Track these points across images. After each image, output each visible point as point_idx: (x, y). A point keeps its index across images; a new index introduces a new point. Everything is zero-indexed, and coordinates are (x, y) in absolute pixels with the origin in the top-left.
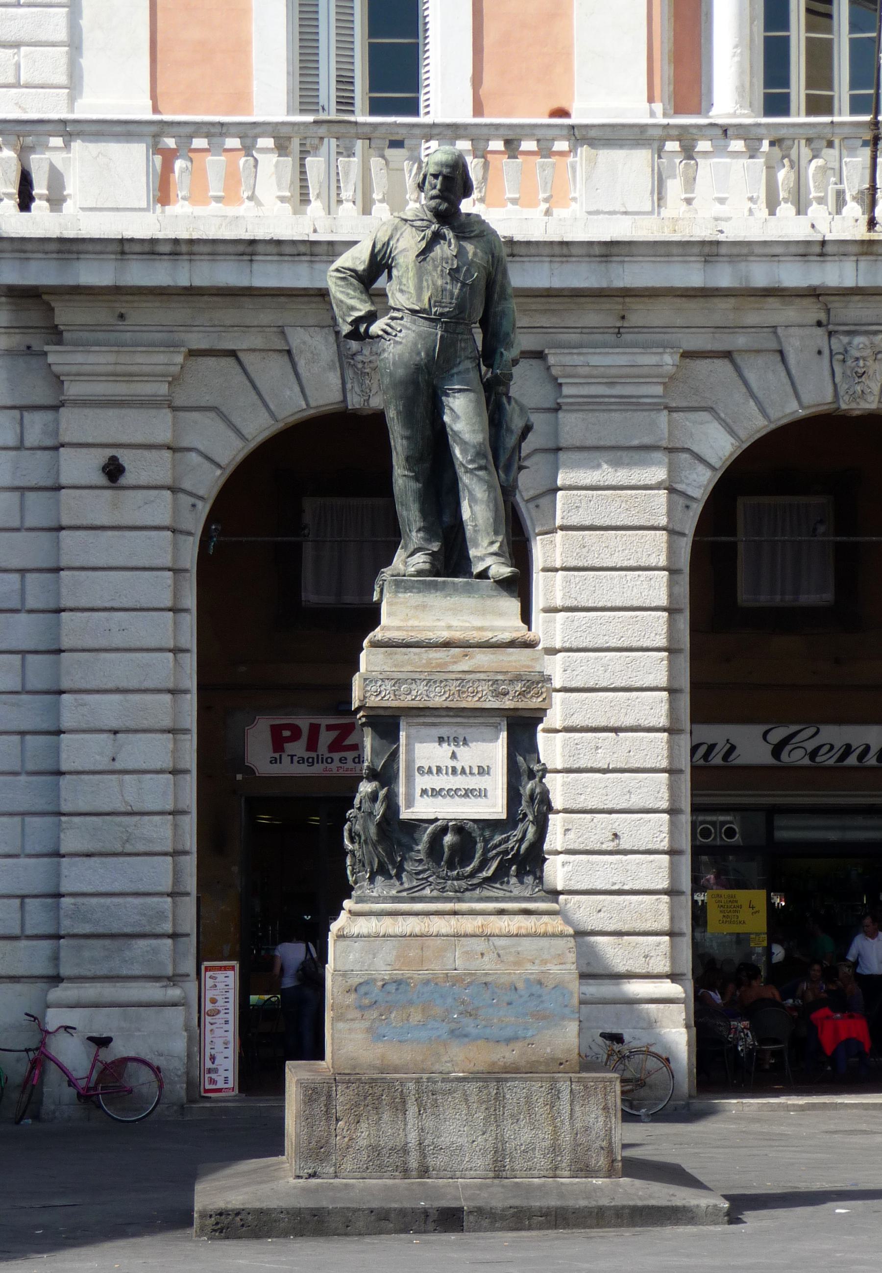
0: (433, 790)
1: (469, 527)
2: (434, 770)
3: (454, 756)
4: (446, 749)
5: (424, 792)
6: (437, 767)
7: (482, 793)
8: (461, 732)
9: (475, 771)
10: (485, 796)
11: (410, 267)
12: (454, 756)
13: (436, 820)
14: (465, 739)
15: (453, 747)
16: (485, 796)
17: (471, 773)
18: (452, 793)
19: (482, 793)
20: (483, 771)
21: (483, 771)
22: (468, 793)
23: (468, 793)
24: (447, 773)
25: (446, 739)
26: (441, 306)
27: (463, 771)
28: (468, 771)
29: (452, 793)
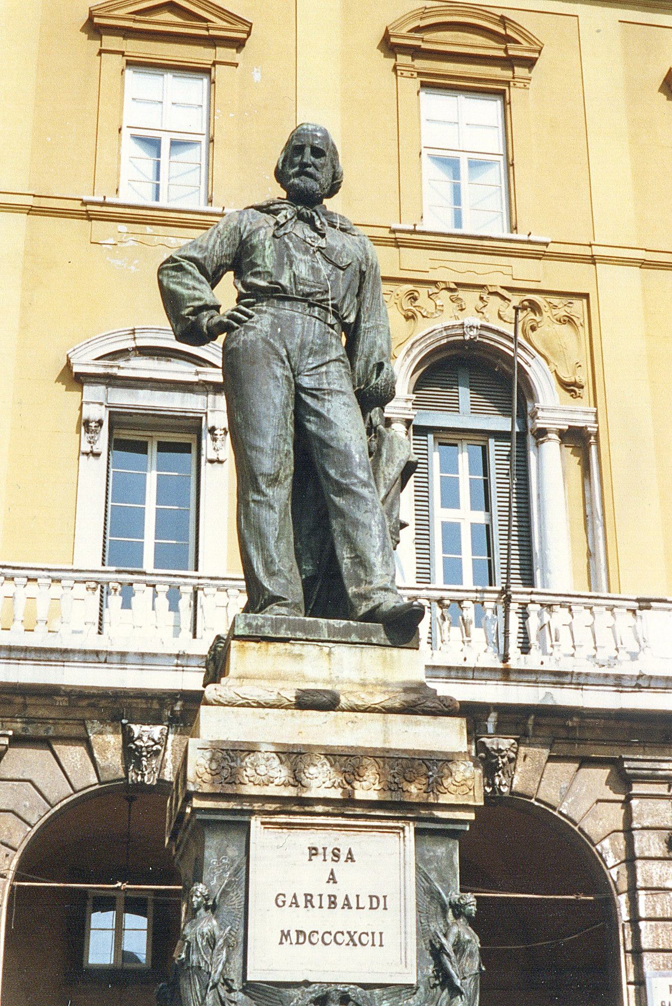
0: (299, 932)
1: (345, 561)
2: (301, 901)
3: (332, 879)
4: (321, 867)
5: (285, 935)
6: (306, 895)
7: (377, 939)
8: (344, 841)
9: (365, 902)
10: (381, 945)
11: (267, 244)
12: (332, 879)
13: (307, 984)
14: (350, 852)
15: (330, 865)
16: (381, 945)
17: (358, 908)
18: (330, 938)
19: (377, 939)
20: (376, 902)
21: (376, 902)
22: (354, 940)
23: (354, 940)
24: (321, 907)
25: (321, 851)
26: (308, 286)
27: (347, 905)
28: (353, 904)
29: (330, 938)
